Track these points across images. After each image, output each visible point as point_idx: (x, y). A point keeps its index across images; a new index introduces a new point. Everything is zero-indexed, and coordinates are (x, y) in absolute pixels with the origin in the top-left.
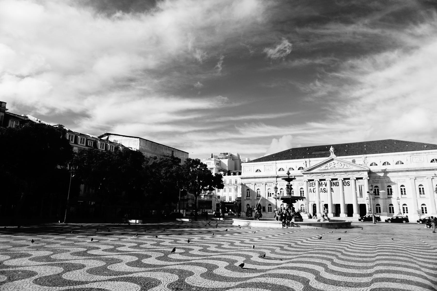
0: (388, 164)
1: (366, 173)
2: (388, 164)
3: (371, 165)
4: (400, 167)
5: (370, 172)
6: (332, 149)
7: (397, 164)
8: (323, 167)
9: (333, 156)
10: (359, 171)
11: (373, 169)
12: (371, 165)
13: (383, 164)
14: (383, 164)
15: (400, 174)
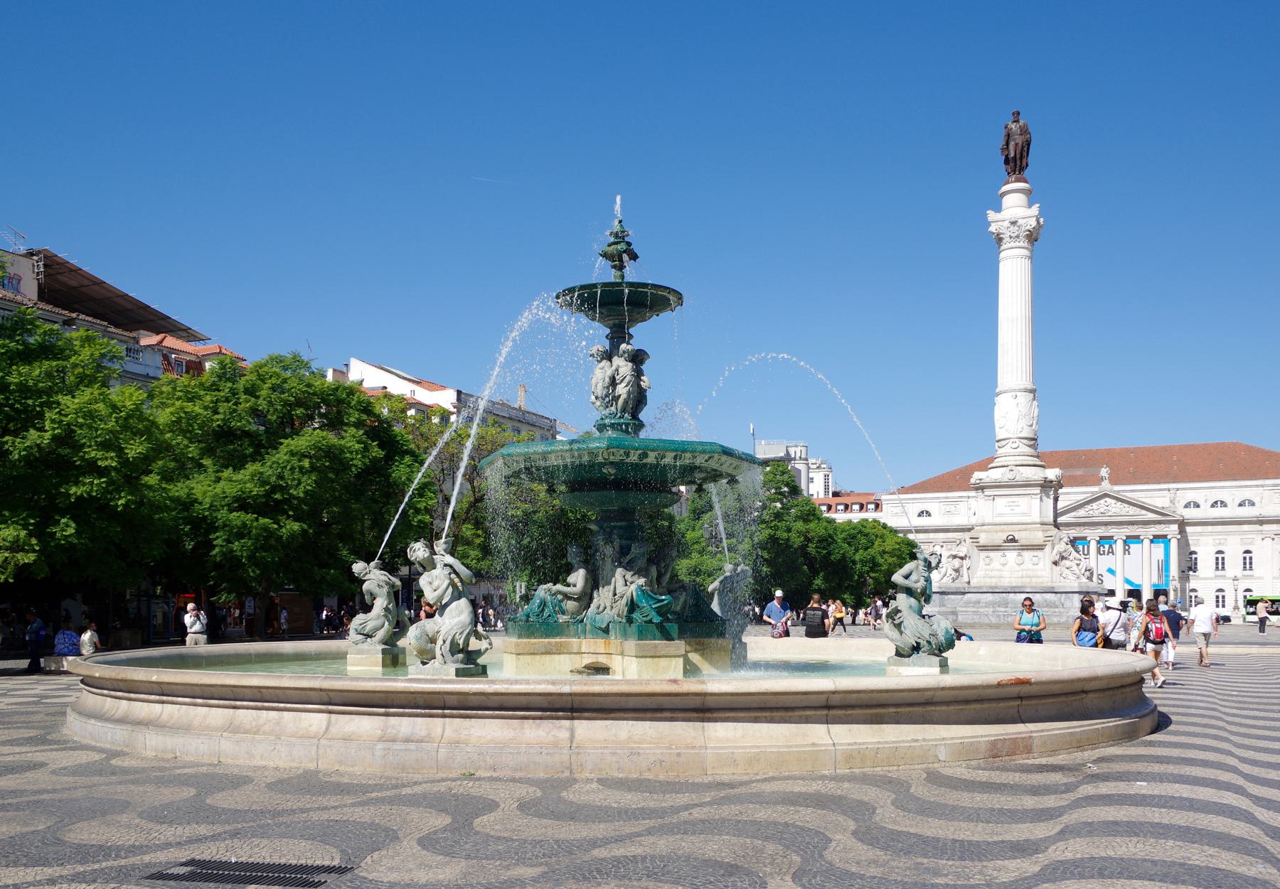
0: (1224, 504)
1: (1175, 527)
2: (1224, 504)
3: (1186, 506)
4: (1247, 512)
5: (1182, 524)
6: (1104, 472)
7: (1240, 505)
8: (1081, 512)
9: (1106, 486)
10: (1160, 522)
11: (1190, 514)
12: (1186, 506)
13: (1213, 506)
14: (1213, 506)
15: (1246, 527)
